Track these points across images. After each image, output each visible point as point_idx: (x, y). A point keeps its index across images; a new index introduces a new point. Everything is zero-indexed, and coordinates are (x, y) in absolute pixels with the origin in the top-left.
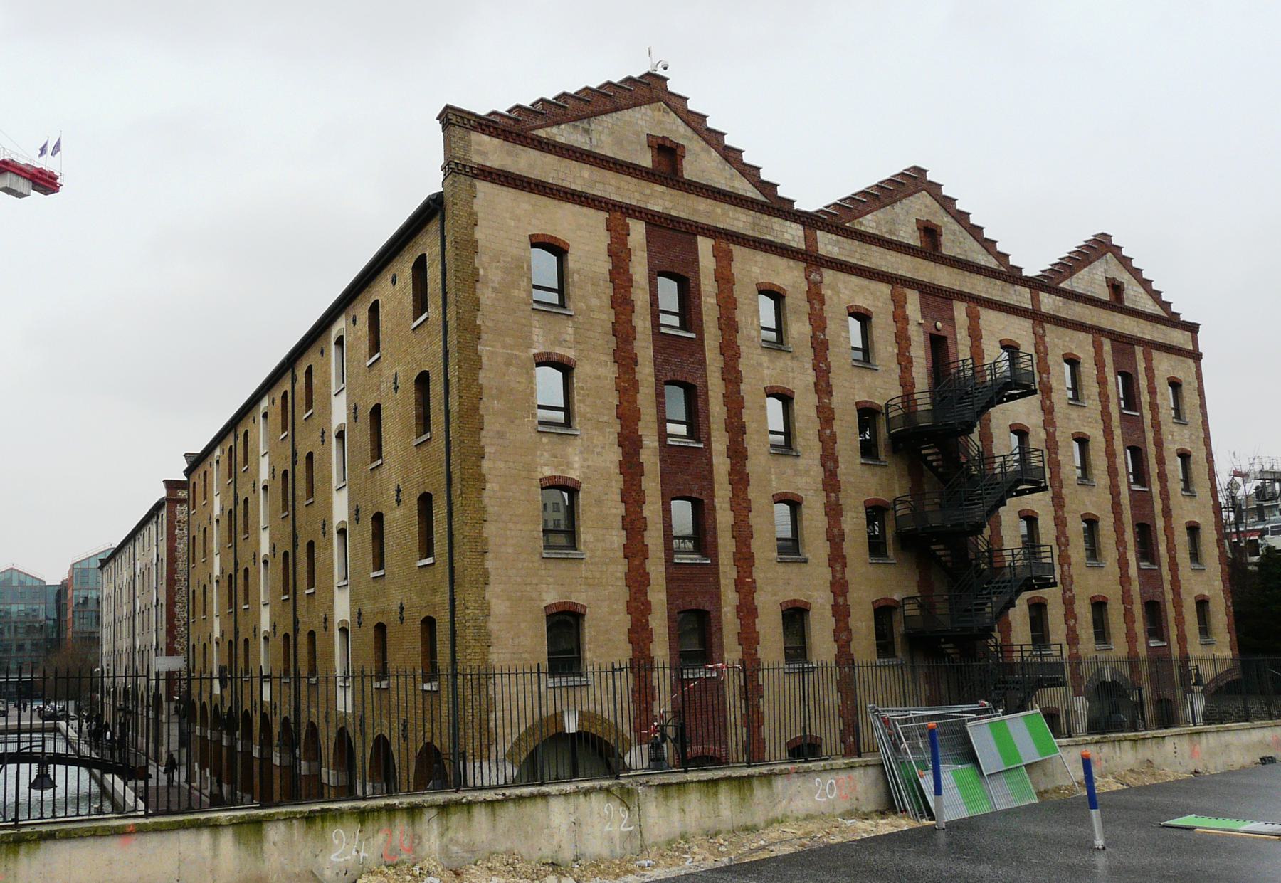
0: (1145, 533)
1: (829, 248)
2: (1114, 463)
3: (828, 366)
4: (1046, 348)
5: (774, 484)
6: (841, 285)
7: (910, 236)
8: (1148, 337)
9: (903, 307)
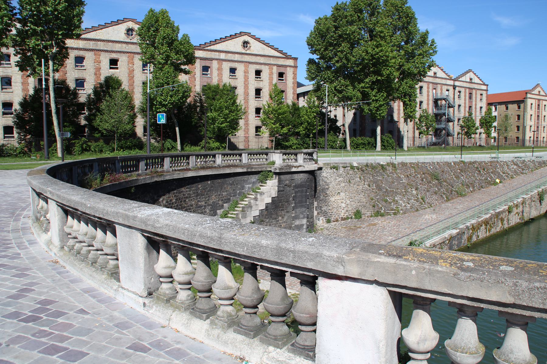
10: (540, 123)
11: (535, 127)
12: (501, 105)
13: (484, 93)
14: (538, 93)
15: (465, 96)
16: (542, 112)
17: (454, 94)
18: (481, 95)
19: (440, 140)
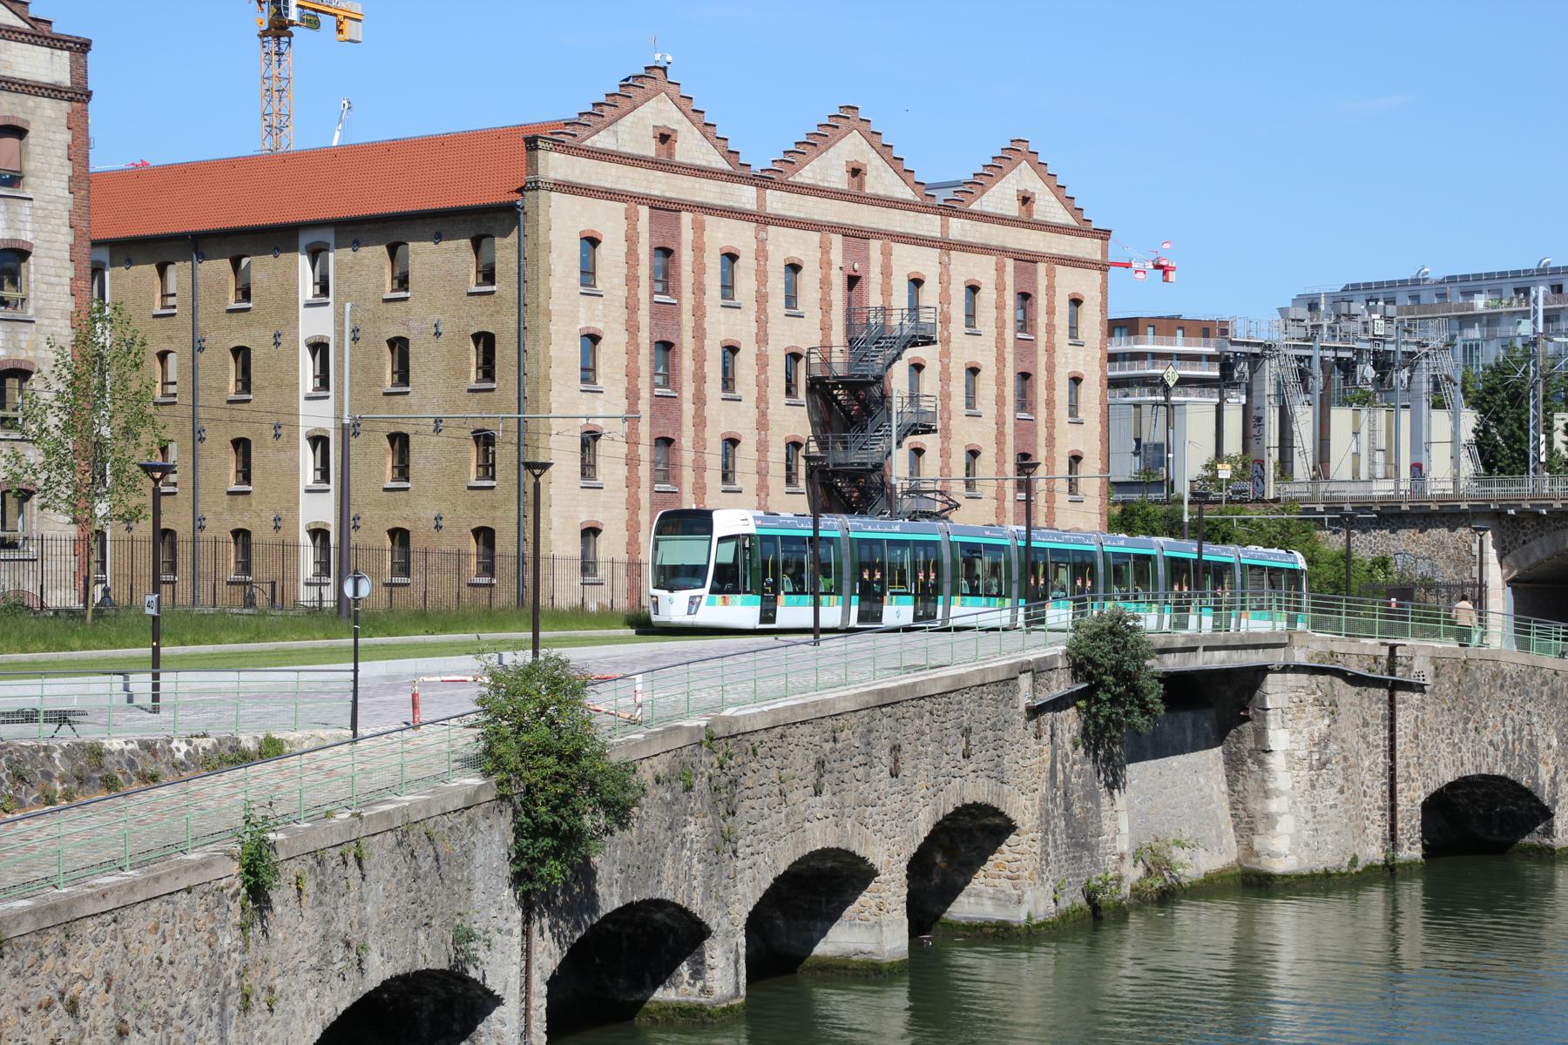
0: (1025, 463)
1: (775, 205)
2: (1003, 391)
3: (767, 317)
4: (949, 276)
5: (723, 425)
6: (781, 239)
7: (840, 181)
8: (1054, 251)
9: (828, 252)
10: (688, 408)
12: (356, 244)
14: (650, 149)
16: (699, 311)
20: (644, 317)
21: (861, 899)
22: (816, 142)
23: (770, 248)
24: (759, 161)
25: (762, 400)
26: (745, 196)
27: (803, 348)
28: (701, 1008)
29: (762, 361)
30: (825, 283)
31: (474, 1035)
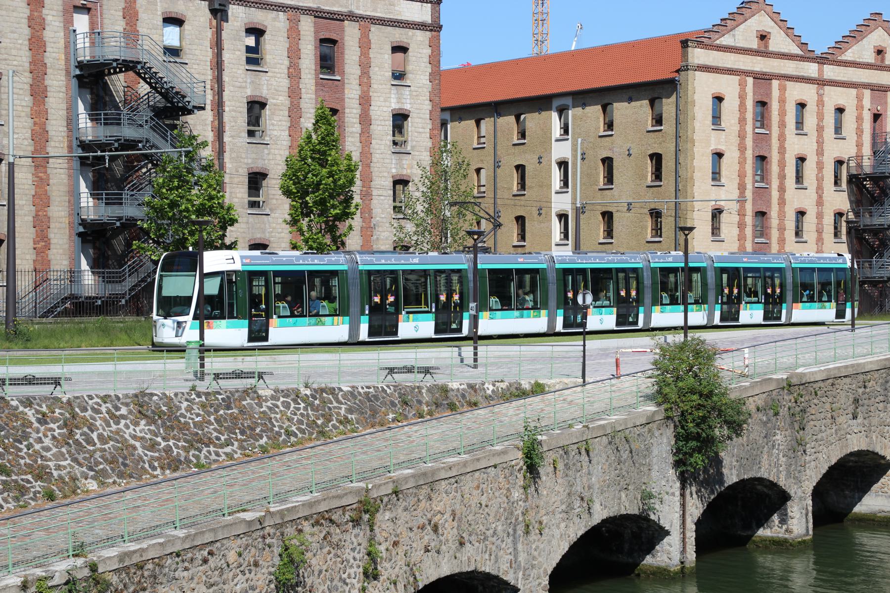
1: (829, 74)
3: (823, 140)
6: (832, 93)
7: (869, 57)
9: (862, 100)
10: (775, 194)
11: (742, 214)
12: (584, 105)
13: (418, 41)
14: (754, 44)
15: (294, 54)
16: (782, 138)
17: (218, 45)
18: (400, 49)
19: (119, 289)
20: (749, 142)
21: (882, 480)
22: (855, 36)
23: (825, 99)
24: (819, 49)
25: (820, 189)
26: (811, 69)
27: (845, 157)
28: (786, 541)
29: (820, 166)
30: (859, 119)
31: (654, 552)
